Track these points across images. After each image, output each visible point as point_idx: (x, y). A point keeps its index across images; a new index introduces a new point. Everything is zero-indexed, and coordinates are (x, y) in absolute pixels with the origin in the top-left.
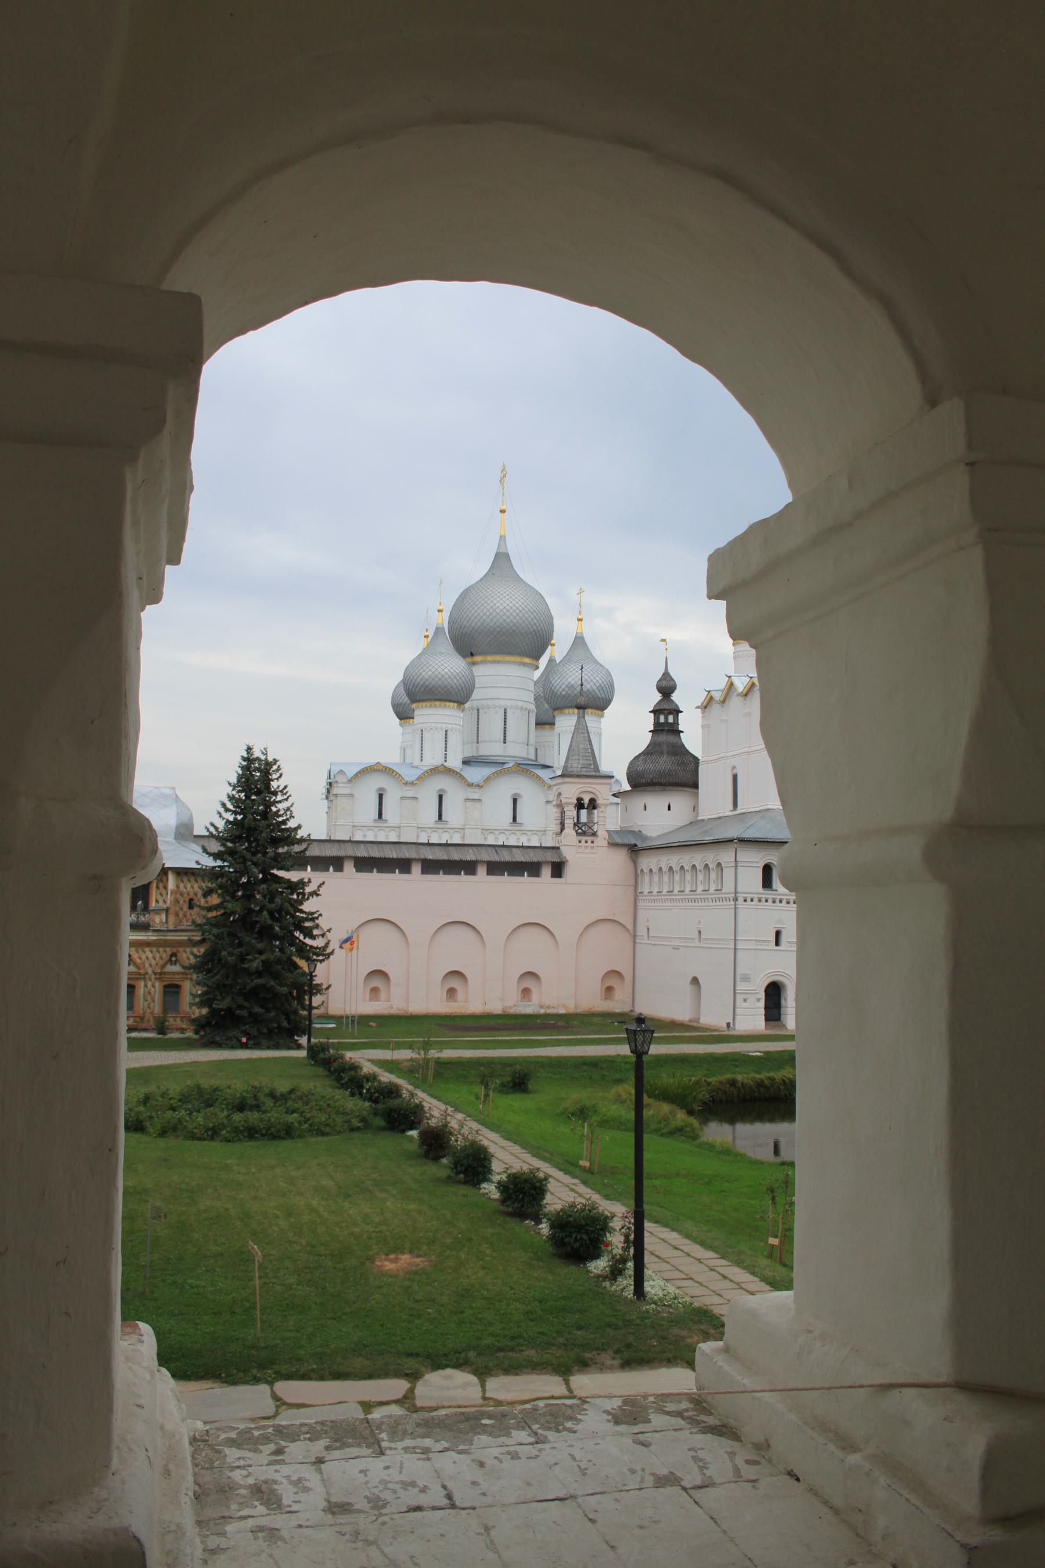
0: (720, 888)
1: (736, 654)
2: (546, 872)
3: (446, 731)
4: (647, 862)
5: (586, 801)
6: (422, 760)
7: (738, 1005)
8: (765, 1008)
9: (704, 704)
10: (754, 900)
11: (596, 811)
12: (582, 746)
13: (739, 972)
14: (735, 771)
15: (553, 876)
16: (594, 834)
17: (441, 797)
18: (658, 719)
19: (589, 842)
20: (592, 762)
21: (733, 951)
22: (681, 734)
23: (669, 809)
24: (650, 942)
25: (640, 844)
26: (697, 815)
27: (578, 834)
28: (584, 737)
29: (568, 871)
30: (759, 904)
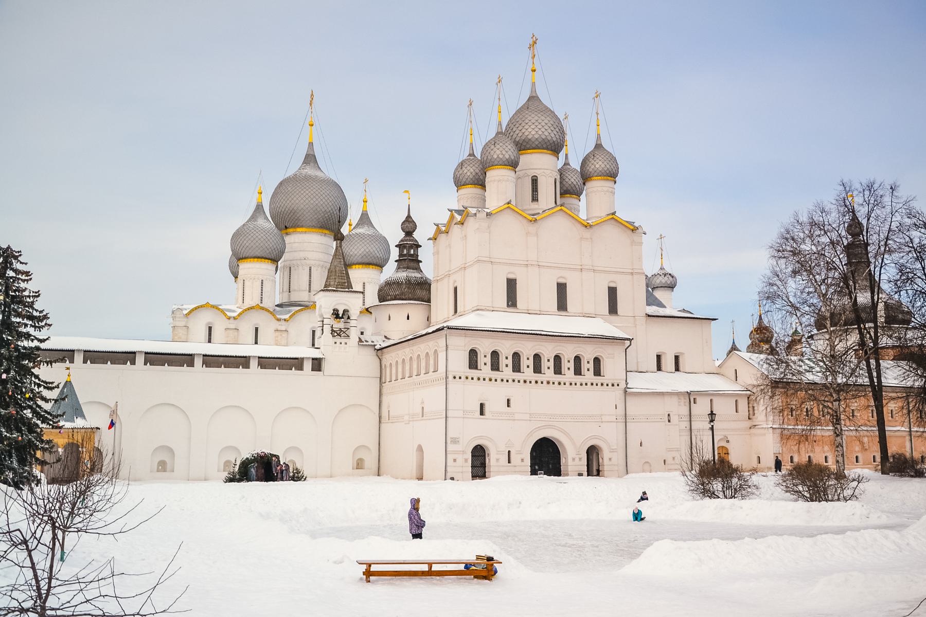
2: (308, 365)
5: (341, 313)
6: (243, 302)
7: (448, 464)
12: (338, 269)
13: (450, 435)
14: (455, 285)
18: (403, 251)
20: (346, 281)
22: (420, 264)
23: (408, 319)
27: (334, 336)
28: (340, 262)
29: (325, 365)
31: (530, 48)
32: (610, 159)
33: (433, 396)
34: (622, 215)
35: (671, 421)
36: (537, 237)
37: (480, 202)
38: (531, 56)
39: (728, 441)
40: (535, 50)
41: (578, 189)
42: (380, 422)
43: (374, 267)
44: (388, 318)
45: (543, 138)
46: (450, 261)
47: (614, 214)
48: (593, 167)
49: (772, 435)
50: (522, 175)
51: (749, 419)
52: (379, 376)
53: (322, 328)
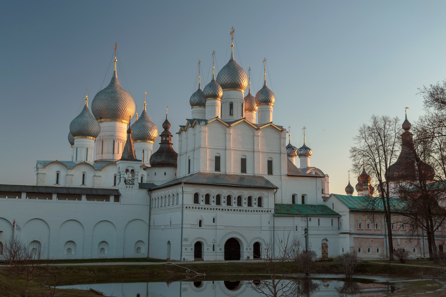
2: (112, 198)
3: (87, 148)
4: (155, 194)
6: (76, 160)
7: (183, 251)
13: (184, 237)
15: (114, 202)
16: (133, 184)
17: (84, 175)
19: (131, 187)
23: (165, 174)
24: (154, 228)
25: (152, 188)
26: (176, 177)
27: (126, 184)
29: (121, 199)
33: (176, 216)
35: (298, 230)
38: (231, 38)
39: (327, 240)
40: (233, 36)
42: (149, 229)
44: (154, 174)
46: (187, 145)
49: (349, 237)
50: (225, 102)
51: (339, 229)
52: (149, 205)
53: (120, 179)
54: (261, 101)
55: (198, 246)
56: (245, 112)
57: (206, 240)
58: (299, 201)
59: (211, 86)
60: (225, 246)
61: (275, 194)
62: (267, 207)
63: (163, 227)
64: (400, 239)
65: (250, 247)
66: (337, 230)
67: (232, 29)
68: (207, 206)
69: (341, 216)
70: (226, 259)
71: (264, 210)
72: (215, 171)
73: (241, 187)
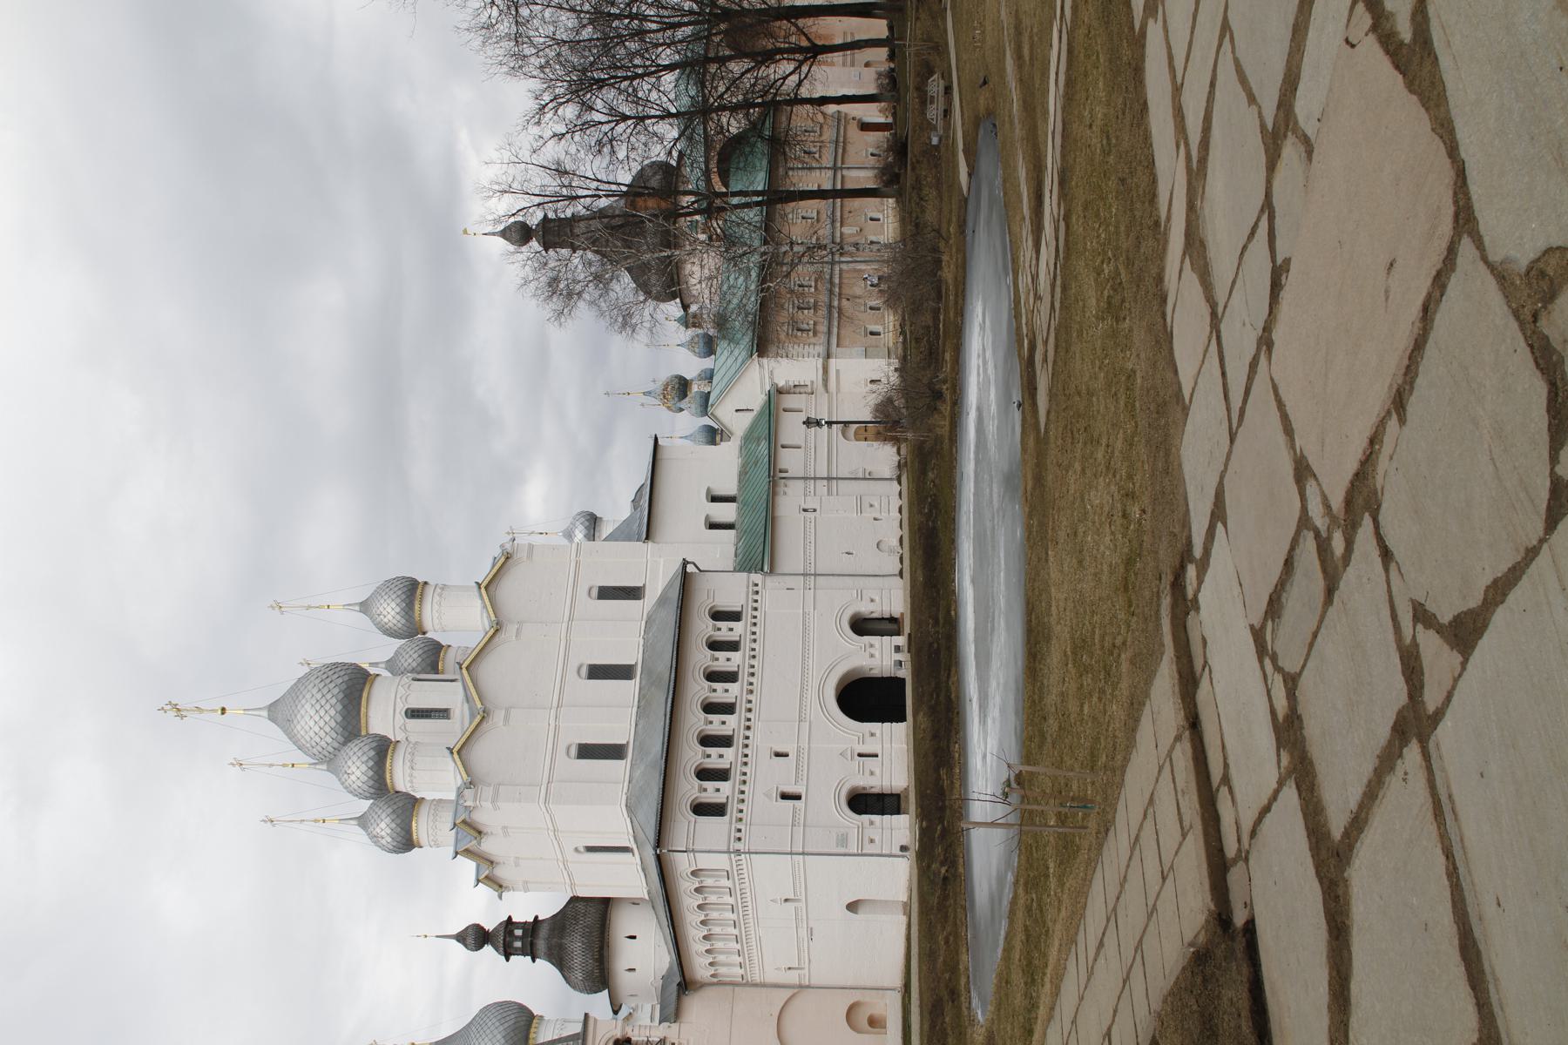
0: (726, 873)
1: (432, 843)
4: (700, 968)
7: (879, 852)
8: (883, 814)
9: (497, 887)
10: (739, 827)
11: (633, 1039)
14: (582, 850)
18: (516, 949)
21: (806, 856)
22: (540, 918)
23: (634, 937)
25: (678, 979)
26: (642, 899)
30: (744, 821)
31: (182, 717)
32: (387, 590)
34: (483, 572)
35: (814, 507)
36: (511, 708)
37: (443, 807)
40: (188, 706)
41: (431, 647)
43: (532, 1030)
44: (631, 973)
45: (345, 687)
47: (479, 585)
48: (398, 617)
51: (812, 394)
52: (731, 987)
54: (407, 617)
55: (862, 802)
56: (443, 673)
57: (841, 781)
58: (727, 512)
59: (346, 772)
60: (863, 722)
61: (700, 571)
62: (743, 595)
63: (803, 933)
64: (842, 226)
65: (867, 647)
66: (816, 396)
67: (165, 712)
68: (736, 776)
69: (774, 385)
70: (901, 718)
71: (751, 604)
72: (623, 759)
73: (676, 668)
